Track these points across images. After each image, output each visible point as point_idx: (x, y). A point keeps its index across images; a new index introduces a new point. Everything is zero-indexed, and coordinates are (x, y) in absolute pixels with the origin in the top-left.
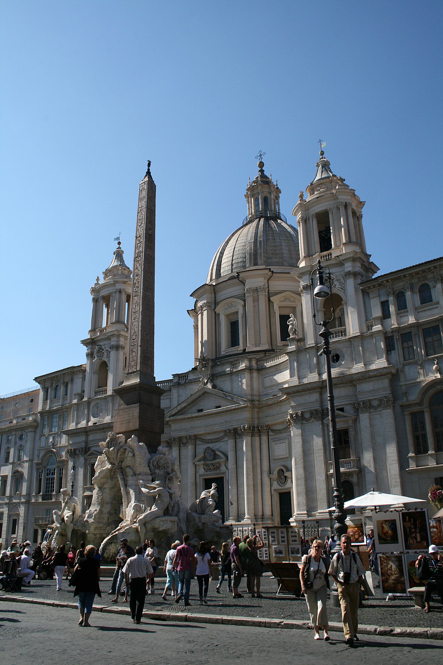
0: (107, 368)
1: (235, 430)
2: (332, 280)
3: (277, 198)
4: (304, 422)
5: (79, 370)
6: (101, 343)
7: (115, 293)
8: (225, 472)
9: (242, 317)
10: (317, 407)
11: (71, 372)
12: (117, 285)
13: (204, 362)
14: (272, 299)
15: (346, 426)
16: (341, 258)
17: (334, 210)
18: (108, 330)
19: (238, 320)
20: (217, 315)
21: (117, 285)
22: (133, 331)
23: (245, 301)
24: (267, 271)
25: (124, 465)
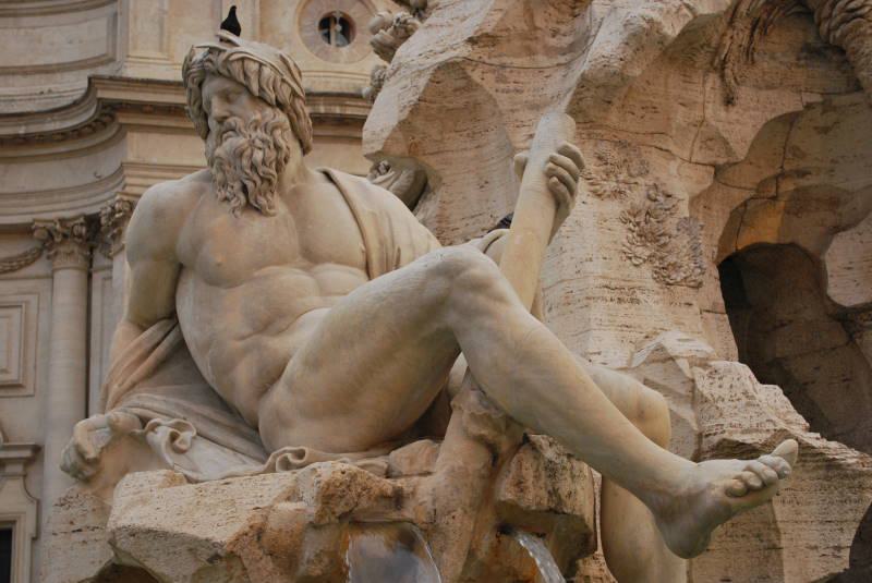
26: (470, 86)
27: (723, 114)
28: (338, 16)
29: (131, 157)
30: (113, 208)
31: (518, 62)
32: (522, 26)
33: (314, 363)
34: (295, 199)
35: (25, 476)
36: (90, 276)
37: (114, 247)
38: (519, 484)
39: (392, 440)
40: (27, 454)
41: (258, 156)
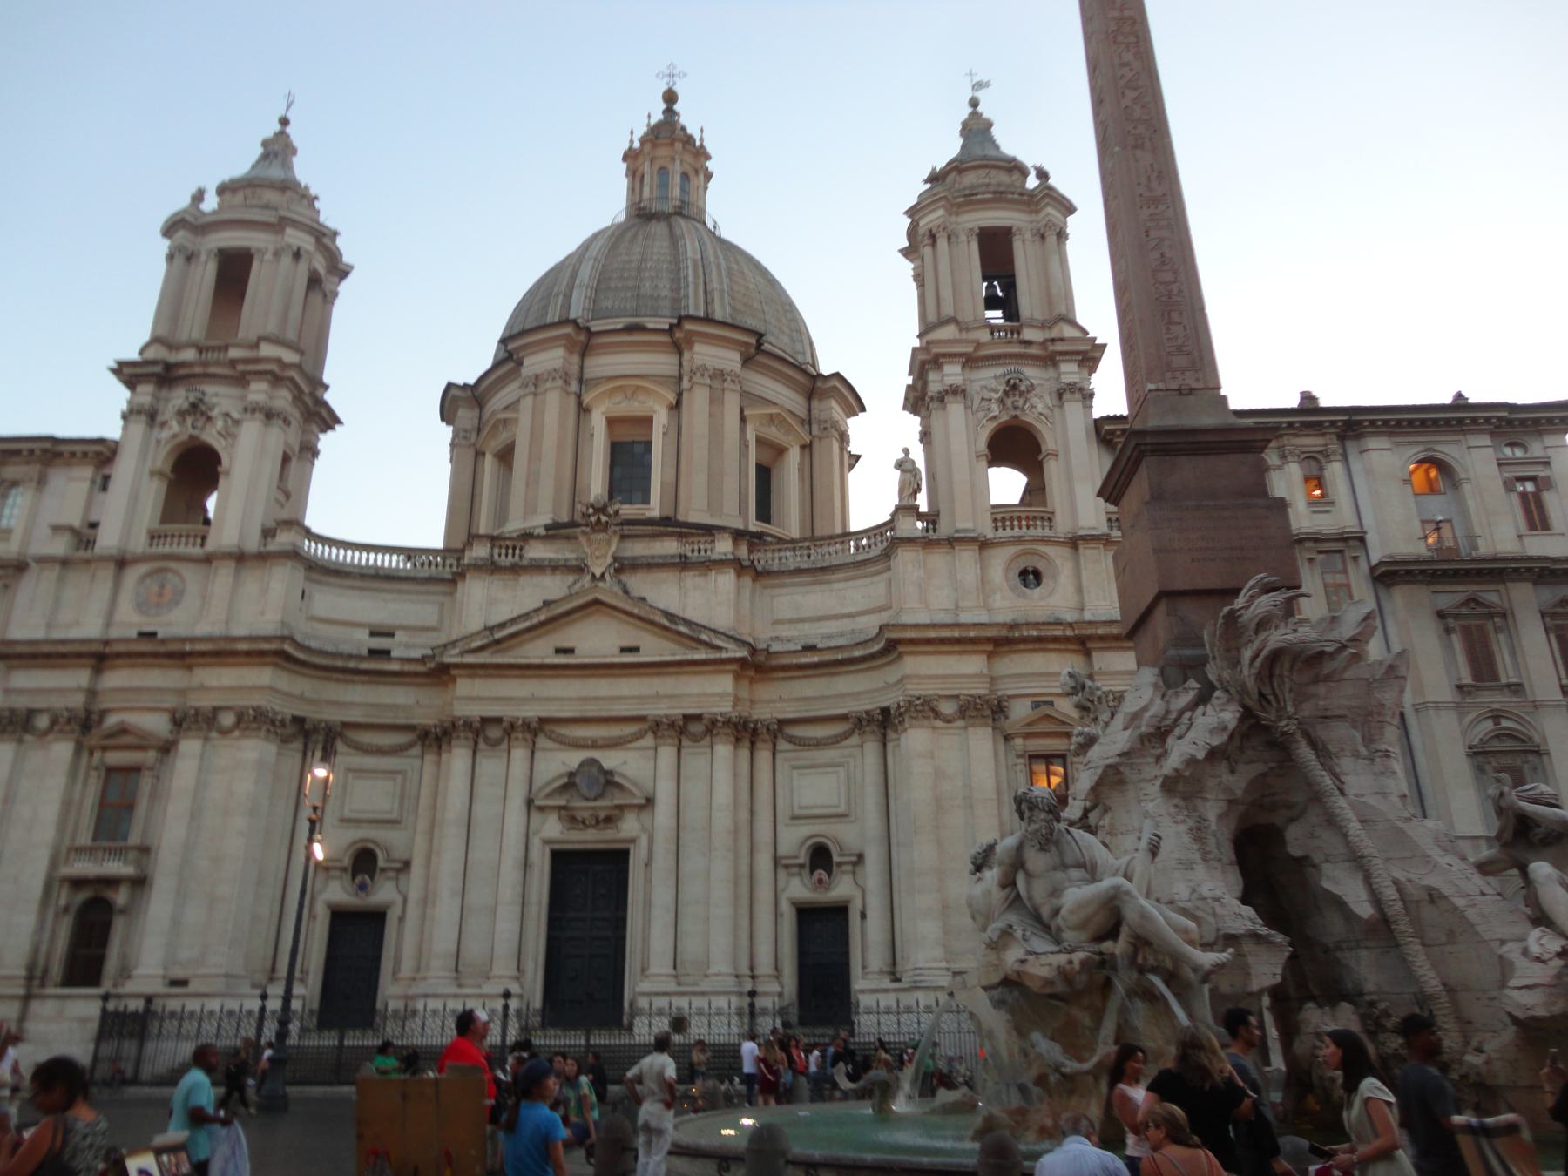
0: (219, 469)
1: (688, 718)
2: (1028, 392)
3: (706, 188)
4: (939, 723)
5: (85, 454)
6: (210, 389)
7: (277, 254)
8: (639, 837)
9: (664, 434)
10: (982, 689)
11: (45, 451)
12: (289, 231)
13: (604, 519)
14: (746, 413)
15: (1064, 747)
16: (1059, 347)
17: (1028, 236)
18: (234, 353)
19: (651, 442)
20: (582, 413)
21: (289, 231)
22: (1155, 255)
23: (680, 395)
24: (753, 341)
25: (1307, 710)
26: (1119, 772)
27: (1231, 778)
28: (1030, 569)
29: (908, 671)
30: (899, 705)
31: (1142, 760)
32: (1139, 746)
33: (1072, 912)
34: (1057, 843)
35: (854, 873)
36: (885, 745)
37: (900, 728)
38: (1145, 959)
39: (1099, 938)
40: (854, 859)
41: (1044, 832)
